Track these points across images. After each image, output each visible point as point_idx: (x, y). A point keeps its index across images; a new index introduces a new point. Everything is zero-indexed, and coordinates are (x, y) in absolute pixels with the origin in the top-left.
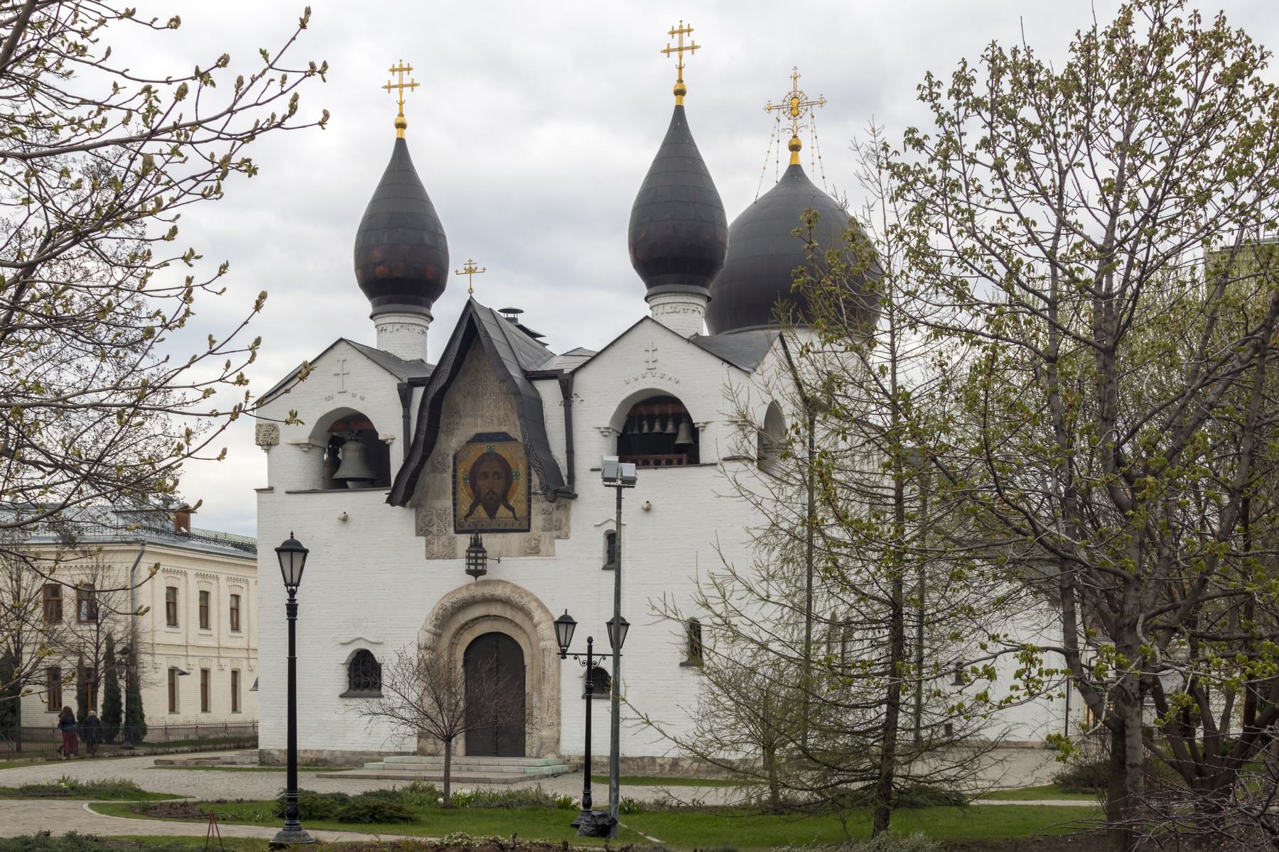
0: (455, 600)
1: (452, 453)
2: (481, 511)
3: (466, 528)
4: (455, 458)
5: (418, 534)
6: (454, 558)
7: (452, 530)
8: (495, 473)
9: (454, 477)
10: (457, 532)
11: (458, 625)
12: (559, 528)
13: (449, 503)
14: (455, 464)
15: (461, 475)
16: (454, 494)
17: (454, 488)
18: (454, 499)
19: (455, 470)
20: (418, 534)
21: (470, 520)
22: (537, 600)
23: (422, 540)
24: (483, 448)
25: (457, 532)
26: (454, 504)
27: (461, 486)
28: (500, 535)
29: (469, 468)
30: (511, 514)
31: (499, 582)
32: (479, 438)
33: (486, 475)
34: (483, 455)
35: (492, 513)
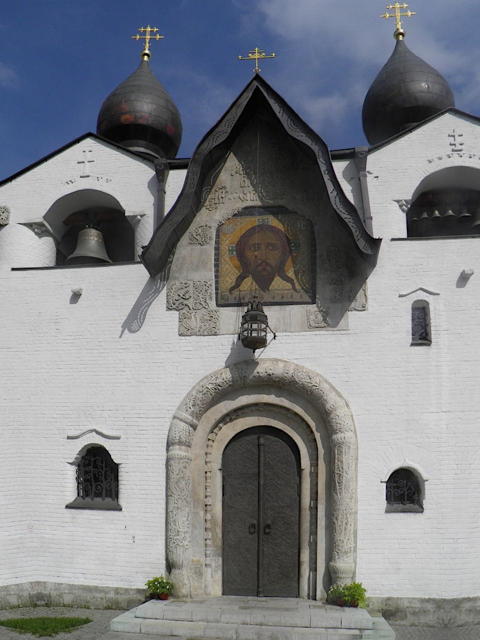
0: (219, 381)
1: (215, 226)
2: (248, 284)
3: (232, 301)
4: (218, 231)
5: (169, 309)
6: (215, 334)
7: (214, 302)
8: (269, 244)
9: (217, 249)
10: (218, 305)
11: (219, 416)
12: (351, 297)
13: (212, 274)
14: (218, 236)
15: (226, 245)
16: (216, 266)
17: (217, 260)
18: (217, 271)
19: (217, 243)
20: (169, 309)
21: (236, 293)
22: (326, 381)
23: (175, 315)
24: (254, 221)
25: (218, 305)
26: (216, 277)
27: (226, 257)
28: (277, 308)
29: (236, 240)
30: (289, 285)
31: (277, 360)
32: (248, 211)
33: (258, 247)
34: (254, 228)
35: (264, 283)
